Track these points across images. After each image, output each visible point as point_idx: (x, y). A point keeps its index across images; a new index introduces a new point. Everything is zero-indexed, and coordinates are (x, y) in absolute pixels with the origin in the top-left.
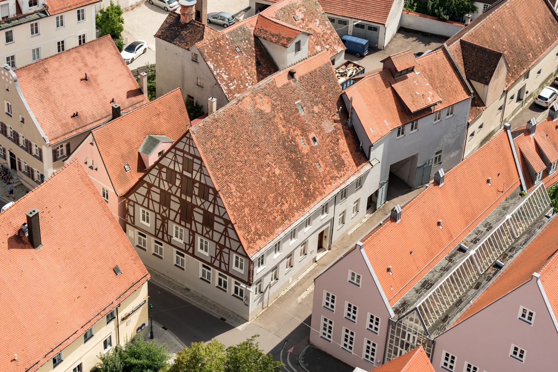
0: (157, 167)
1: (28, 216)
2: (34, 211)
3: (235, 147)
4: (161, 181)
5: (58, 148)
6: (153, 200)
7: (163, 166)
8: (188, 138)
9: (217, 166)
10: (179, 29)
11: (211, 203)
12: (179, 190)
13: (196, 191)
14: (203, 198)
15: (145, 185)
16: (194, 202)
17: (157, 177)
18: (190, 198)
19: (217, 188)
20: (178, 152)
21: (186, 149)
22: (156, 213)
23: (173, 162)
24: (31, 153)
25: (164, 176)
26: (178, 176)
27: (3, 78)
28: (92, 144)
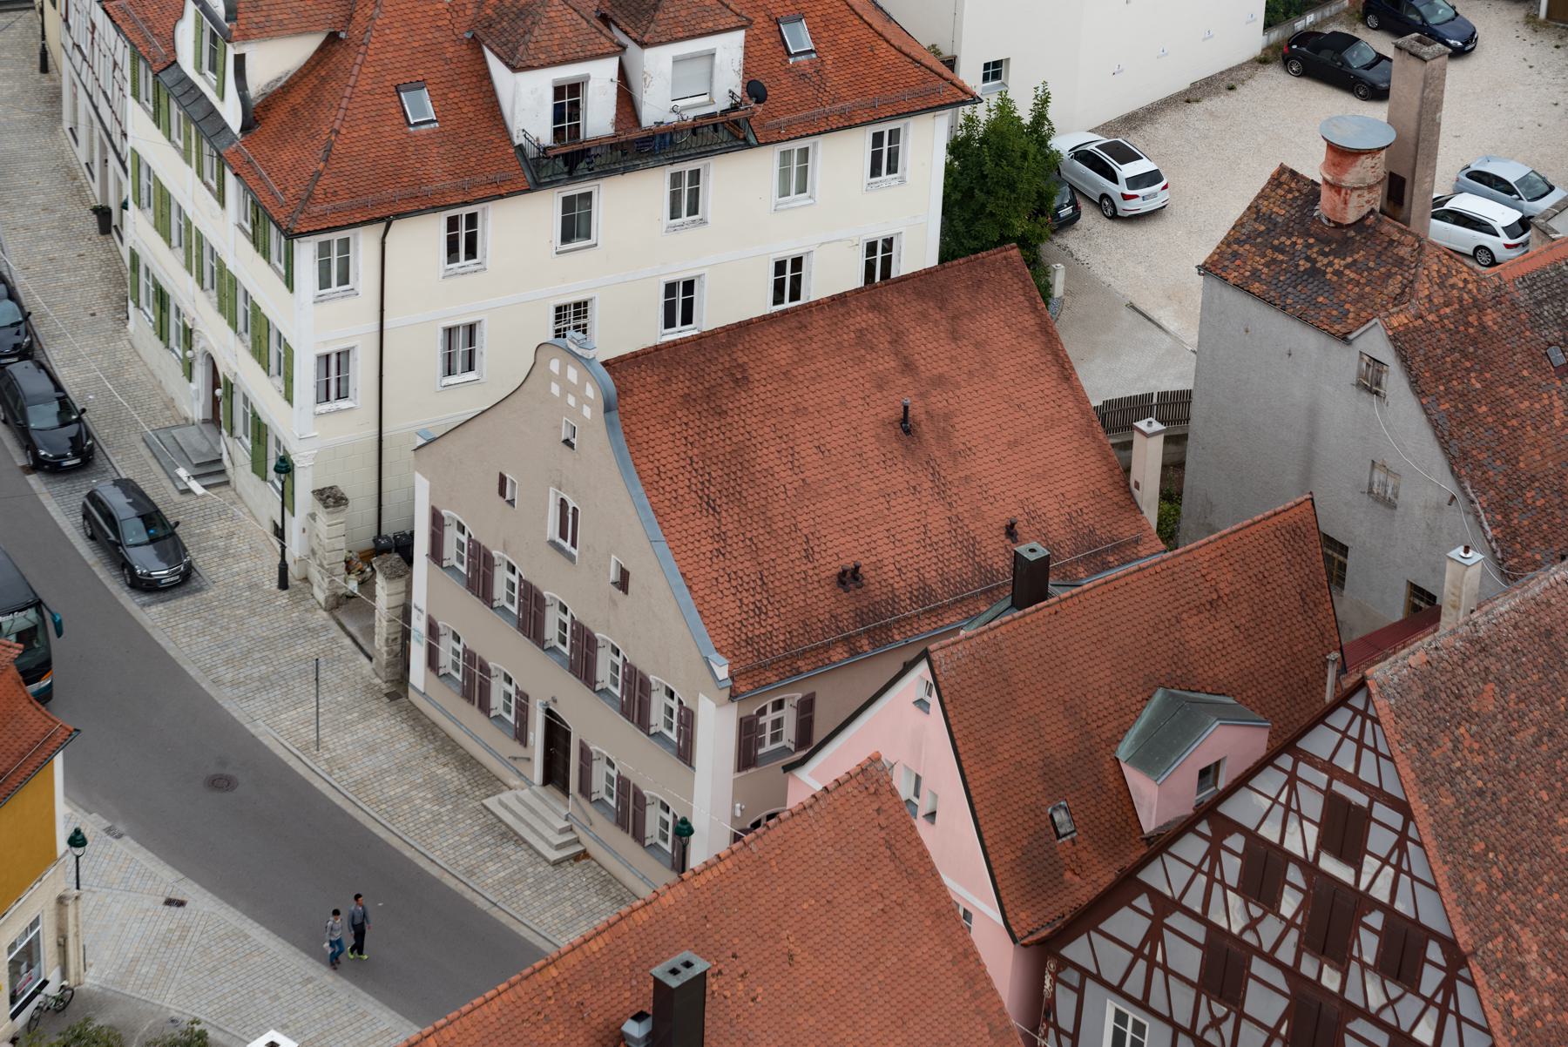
0: (1204, 827)
1: (657, 981)
2: (688, 965)
3: (1550, 768)
4: (1217, 889)
5: (762, 712)
6: (1167, 971)
7: (1236, 827)
8: (1356, 712)
9: (1470, 843)
10: (1309, 246)
11: (1429, 1002)
12: (1293, 935)
13: (1369, 946)
14: (1397, 978)
15: (1143, 902)
16: (1354, 995)
17: (1198, 869)
18: (1338, 977)
19: (1464, 938)
20: (1304, 770)
21: (1346, 762)
22: (1177, 1029)
23: (1279, 811)
24: (643, 723)
25: (1232, 867)
26: (1294, 874)
27: (555, 389)
28: (921, 704)
